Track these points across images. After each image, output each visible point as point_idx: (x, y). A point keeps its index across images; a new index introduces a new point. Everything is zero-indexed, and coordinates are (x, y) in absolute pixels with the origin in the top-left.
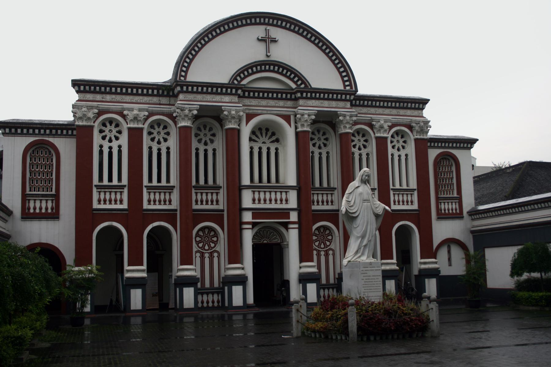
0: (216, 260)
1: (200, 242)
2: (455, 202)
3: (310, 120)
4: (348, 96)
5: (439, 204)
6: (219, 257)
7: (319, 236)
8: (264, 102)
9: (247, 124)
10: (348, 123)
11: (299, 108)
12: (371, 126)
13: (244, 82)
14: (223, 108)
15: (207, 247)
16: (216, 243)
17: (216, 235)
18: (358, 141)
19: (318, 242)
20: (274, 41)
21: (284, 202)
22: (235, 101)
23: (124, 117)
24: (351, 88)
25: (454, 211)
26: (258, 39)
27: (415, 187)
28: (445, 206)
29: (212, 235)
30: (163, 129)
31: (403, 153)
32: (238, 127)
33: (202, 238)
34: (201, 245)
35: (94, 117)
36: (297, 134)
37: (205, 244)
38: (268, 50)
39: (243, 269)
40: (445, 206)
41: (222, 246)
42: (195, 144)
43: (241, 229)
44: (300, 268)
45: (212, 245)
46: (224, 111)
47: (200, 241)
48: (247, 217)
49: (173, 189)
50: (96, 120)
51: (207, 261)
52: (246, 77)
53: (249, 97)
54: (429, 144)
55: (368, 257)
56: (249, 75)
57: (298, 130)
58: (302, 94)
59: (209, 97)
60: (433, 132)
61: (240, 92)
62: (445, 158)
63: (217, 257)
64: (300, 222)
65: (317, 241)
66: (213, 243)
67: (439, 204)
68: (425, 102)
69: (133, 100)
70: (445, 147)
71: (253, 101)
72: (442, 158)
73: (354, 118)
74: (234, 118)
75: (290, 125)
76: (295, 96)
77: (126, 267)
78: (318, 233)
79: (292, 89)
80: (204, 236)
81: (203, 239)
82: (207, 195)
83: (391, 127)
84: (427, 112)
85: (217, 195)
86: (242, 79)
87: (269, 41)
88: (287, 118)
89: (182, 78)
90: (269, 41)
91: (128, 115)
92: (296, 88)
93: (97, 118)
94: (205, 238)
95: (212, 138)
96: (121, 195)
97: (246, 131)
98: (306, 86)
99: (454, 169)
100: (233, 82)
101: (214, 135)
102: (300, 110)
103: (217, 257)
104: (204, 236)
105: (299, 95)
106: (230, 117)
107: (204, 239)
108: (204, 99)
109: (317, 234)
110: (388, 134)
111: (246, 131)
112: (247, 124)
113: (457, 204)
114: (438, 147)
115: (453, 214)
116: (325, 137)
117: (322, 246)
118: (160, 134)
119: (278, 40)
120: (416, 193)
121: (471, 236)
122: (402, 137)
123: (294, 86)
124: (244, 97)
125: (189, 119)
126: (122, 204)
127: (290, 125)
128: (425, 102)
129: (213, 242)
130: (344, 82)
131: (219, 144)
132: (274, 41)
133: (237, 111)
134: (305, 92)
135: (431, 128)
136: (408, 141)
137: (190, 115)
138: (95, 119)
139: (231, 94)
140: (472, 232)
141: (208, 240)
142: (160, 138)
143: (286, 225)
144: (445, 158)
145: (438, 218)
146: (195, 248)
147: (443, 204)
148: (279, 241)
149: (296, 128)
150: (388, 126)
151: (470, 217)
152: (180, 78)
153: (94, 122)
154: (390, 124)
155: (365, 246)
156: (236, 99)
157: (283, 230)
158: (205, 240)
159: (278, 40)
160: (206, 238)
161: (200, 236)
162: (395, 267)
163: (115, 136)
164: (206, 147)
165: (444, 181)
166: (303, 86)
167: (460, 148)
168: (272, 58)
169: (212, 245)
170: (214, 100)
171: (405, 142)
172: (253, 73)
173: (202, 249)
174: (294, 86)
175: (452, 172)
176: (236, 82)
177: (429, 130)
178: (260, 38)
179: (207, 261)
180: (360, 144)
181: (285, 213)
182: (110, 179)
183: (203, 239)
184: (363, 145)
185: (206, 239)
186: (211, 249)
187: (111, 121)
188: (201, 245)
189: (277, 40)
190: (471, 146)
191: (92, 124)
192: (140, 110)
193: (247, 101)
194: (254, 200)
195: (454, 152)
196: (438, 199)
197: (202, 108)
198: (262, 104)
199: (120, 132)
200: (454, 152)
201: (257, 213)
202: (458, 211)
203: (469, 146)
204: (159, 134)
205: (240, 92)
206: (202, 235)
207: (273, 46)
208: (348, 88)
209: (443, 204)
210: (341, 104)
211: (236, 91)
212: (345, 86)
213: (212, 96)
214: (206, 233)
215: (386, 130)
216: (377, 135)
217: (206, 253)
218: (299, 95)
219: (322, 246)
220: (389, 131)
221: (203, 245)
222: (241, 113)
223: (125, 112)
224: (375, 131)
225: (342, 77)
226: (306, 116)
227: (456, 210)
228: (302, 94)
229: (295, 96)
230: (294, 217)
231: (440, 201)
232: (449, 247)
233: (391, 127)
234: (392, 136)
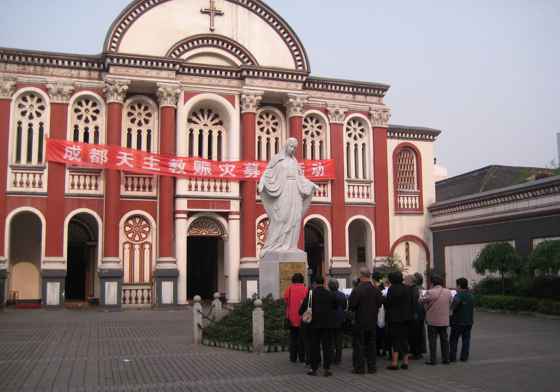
0: (147, 252)
1: (130, 232)
2: (415, 197)
3: (257, 101)
5: (398, 198)
6: (151, 249)
7: (264, 229)
8: (206, 80)
9: (185, 103)
10: (298, 105)
11: (244, 87)
12: (326, 112)
13: (184, 56)
14: (157, 83)
15: (137, 238)
16: (147, 233)
17: (148, 224)
18: (312, 127)
19: (263, 235)
20: (220, 14)
22: (172, 77)
23: (47, 90)
24: (304, 68)
25: (414, 207)
26: (201, 11)
27: (373, 179)
28: (404, 201)
29: (144, 225)
30: (92, 106)
31: (360, 142)
32: (175, 106)
33: (132, 228)
34: (130, 235)
35: (11, 89)
36: (243, 117)
37: (136, 235)
38: (212, 23)
39: (175, 262)
40: (404, 201)
41: (153, 238)
42: (126, 123)
43: (175, 219)
44: (241, 263)
45: (144, 236)
46: (158, 87)
47: (129, 230)
48: (182, 205)
49: (100, 173)
50: (14, 93)
51: (137, 253)
52: (185, 51)
53: (189, 74)
54: (388, 134)
55: (291, 247)
56: (190, 49)
57: (242, 112)
58: (248, 72)
59: (143, 72)
60: (394, 121)
61: (177, 67)
62: (406, 150)
63: (149, 249)
64: (242, 212)
65: (261, 235)
66: (144, 233)
67: (398, 198)
68: (385, 88)
69: (58, 73)
70: (406, 138)
71: (194, 79)
72: (403, 150)
73: (306, 101)
74: (169, 95)
75: (234, 106)
76: (241, 75)
77: (43, 258)
78: (263, 226)
79: (239, 67)
80: (135, 226)
81: (133, 229)
82: (139, 180)
83: (346, 114)
84: (388, 98)
85: (150, 181)
86: (182, 54)
88: (231, 99)
89: (113, 50)
91: (50, 89)
92: (241, 66)
93: (15, 91)
94: (135, 227)
95: (147, 118)
96: (40, 177)
97: (184, 110)
98: (253, 63)
100: (170, 56)
101: (149, 115)
102: (245, 89)
103: (149, 249)
104: (135, 226)
105: (245, 73)
106: (166, 95)
107: (134, 229)
108: (137, 73)
109: (262, 227)
110: (344, 121)
111: (184, 110)
112: (185, 102)
113: (417, 198)
114: (399, 138)
115: (412, 209)
116: (274, 122)
118: (88, 112)
119: (223, 13)
120: (373, 185)
121: (431, 234)
122: (360, 125)
123: (239, 63)
125: (119, 94)
126: (42, 188)
127: (234, 106)
128: (385, 88)
129: (145, 232)
130: (296, 62)
131: (154, 124)
132: (220, 14)
133: (174, 88)
134: (251, 70)
135: (390, 116)
136: (366, 130)
137: (120, 90)
138: (13, 92)
139: (168, 69)
140: (432, 229)
141: (139, 231)
142: (88, 116)
143: (226, 215)
145: (396, 214)
146: (123, 238)
147: (402, 198)
148: (220, 234)
149: (241, 109)
150: (344, 112)
151: (431, 213)
153: (12, 95)
154: (346, 110)
155: (288, 233)
156: (173, 75)
157: (222, 220)
158: (135, 230)
159: (223, 13)
160: (137, 228)
161: (130, 226)
162: (347, 265)
163: (37, 112)
164: (139, 128)
165: (404, 174)
166: (250, 63)
167: (422, 139)
168: (216, 32)
169: (144, 236)
170: (148, 75)
171: (362, 130)
172: (194, 48)
173: (132, 240)
174: (239, 63)
175: (413, 165)
176: (173, 55)
177: (389, 118)
178: (203, 10)
179: (137, 253)
180: (313, 130)
181: (226, 202)
182: (29, 159)
183: (133, 229)
184: (316, 132)
185: (137, 229)
186: (142, 241)
187: (32, 95)
188: (130, 235)
189: (222, 13)
190: (433, 137)
191: (9, 97)
192: (64, 84)
193: (186, 79)
194: (190, 187)
195: (415, 143)
196: (396, 193)
197: (133, 84)
198: (203, 82)
199: (42, 108)
200: (415, 143)
201: (193, 201)
202: (418, 207)
203: (431, 137)
204: (87, 111)
205: (177, 67)
206: (133, 224)
207: (217, 19)
208: (300, 68)
209: (402, 198)
210: (293, 85)
212: (297, 66)
213: (146, 70)
214: (137, 222)
215: (341, 117)
216: (331, 121)
217: (136, 244)
218: (245, 73)
220: (345, 118)
221: (133, 236)
222: (178, 91)
223: (48, 86)
224: (330, 117)
225: (294, 57)
226: (252, 97)
227: (416, 205)
228: (248, 72)
229: (241, 75)
230: (235, 206)
231: (399, 195)
232: (407, 244)
233: (346, 114)
234: (349, 124)
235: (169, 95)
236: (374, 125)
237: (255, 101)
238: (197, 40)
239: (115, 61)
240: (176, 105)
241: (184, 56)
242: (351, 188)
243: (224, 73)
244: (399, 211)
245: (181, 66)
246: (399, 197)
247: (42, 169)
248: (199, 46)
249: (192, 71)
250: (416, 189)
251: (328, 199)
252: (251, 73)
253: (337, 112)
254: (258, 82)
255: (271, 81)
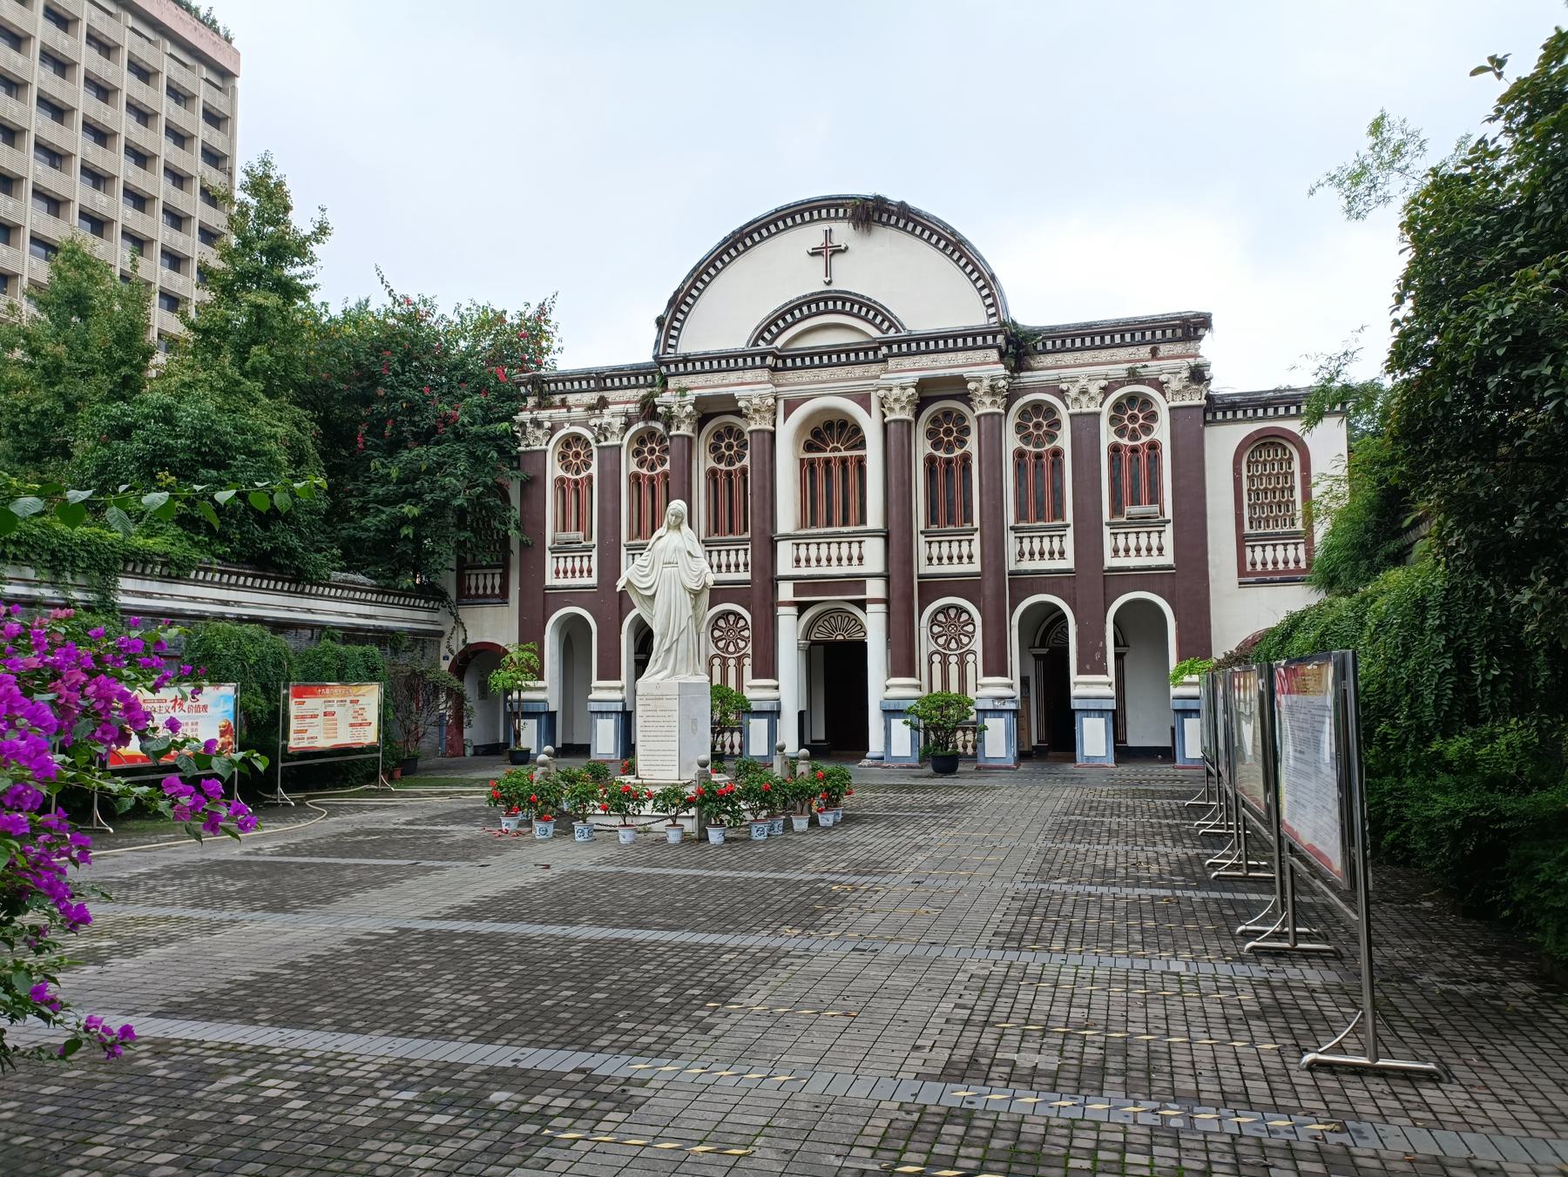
2: (1296, 544)
4: (990, 339)
12: (1061, 394)
13: (779, 343)
15: (731, 649)
21: (855, 561)
39: (777, 688)
44: (887, 687)
48: (786, 591)
58: (890, 348)
59: (716, 378)
61: (769, 360)
72: (1264, 444)
74: (756, 411)
75: (870, 414)
83: (1106, 391)
84: (1209, 348)
86: (775, 337)
87: (829, 252)
88: (864, 400)
90: (829, 252)
93: (551, 436)
97: (787, 434)
99: (1296, 466)
100: (755, 344)
105: (884, 350)
113: (1301, 548)
117: (953, 645)
119: (847, 248)
123: (875, 333)
124: (785, 369)
127: (870, 414)
134: (895, 342)
139: (754, 367)
143: (862, 604)
144: (1272, 443)
149: (884, 416)
152: (664, 350)
153: (547, 444)
154: (1103, 383)
156: (764, 375)
159: (847, 248)
166: (893, 330)
174: (875, 333)
181: (858, 583)
188: (721, 644)
191: (544, 447)
194: (798, 561)
196: (1242, 540)
201: (802, 584)
205: (769, 360)
207: (837, 260)
209: (1258, 550)
210: (978, 356)
211: (763, 359)
219: (953, 645)
224: (1069, 402)
226: (896, 392)
227: (1297, 562)
228: (890, 348)
230: (875, 589)
233: (1106, 391)
235: (756, 411)
236: (1172, 404)
237: (903, 399)
238: (799, 307)
239: (672, 367)
240: (774, 426)
241: (779, 343)
242: (1121, 538)
243: (861, 355)
244: (1250, 577)
245: (776, 357)
246: (1253, 547)
247: (589, 549)
248: (827, 312)
249: (798, 361)
250: (1299, 526)
251: (1068, 563)
252: (895, 347)
253: (1084, 392)
254: (907, 362)
255: (935, 356)
